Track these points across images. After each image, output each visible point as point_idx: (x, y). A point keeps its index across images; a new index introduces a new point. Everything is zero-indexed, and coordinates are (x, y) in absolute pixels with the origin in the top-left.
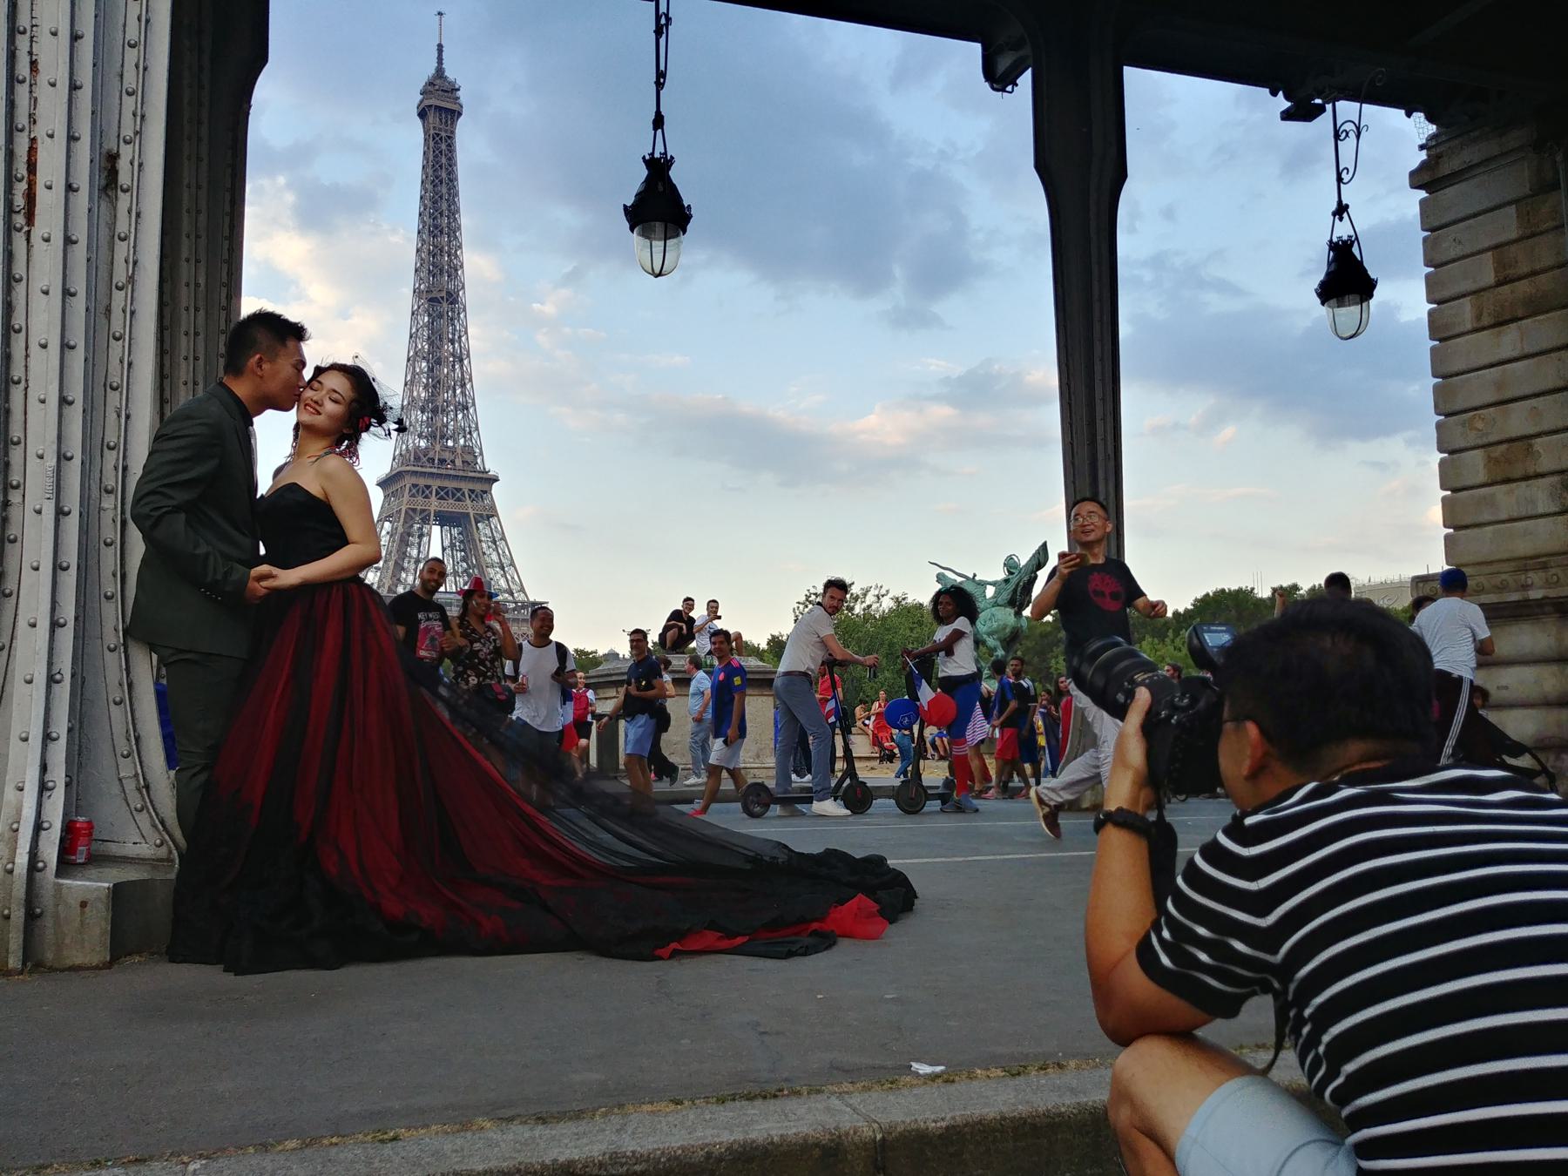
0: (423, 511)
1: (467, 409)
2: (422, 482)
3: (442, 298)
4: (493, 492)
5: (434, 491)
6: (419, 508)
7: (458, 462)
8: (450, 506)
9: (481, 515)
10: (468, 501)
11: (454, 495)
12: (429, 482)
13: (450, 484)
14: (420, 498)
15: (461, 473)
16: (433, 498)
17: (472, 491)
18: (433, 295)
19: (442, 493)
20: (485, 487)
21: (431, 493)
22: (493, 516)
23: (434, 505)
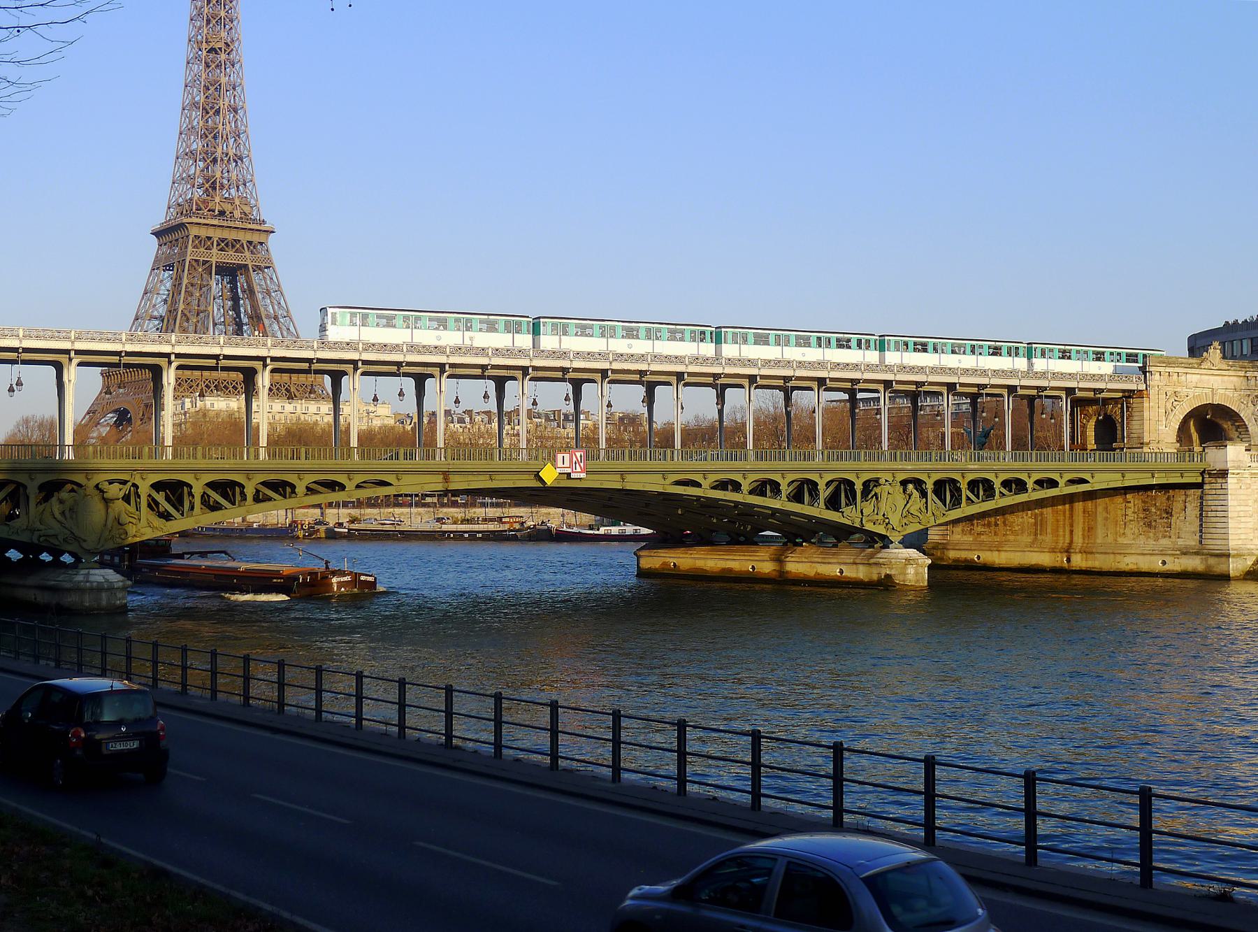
0: (205, 262)
1: (241, 159)
2: (203, 232)
3: (220, 49)
4: (269, 244)
5: (215, 243)
6: (202, 259)
7: (237, 214)
8: (231, 257)
9: (259, 268)
10: (247, 254)
11: (233, 246)
12: (211, 232)
13: (231, 235)
14: (202, 250)
15: (239, 225)
16: (215, 250)
17: (250, 242)
18: (211, 44)
19: (223, 244)
20: (262, 238)
21: (212, 244)
22: (269, 267)
23: (215, 256)
